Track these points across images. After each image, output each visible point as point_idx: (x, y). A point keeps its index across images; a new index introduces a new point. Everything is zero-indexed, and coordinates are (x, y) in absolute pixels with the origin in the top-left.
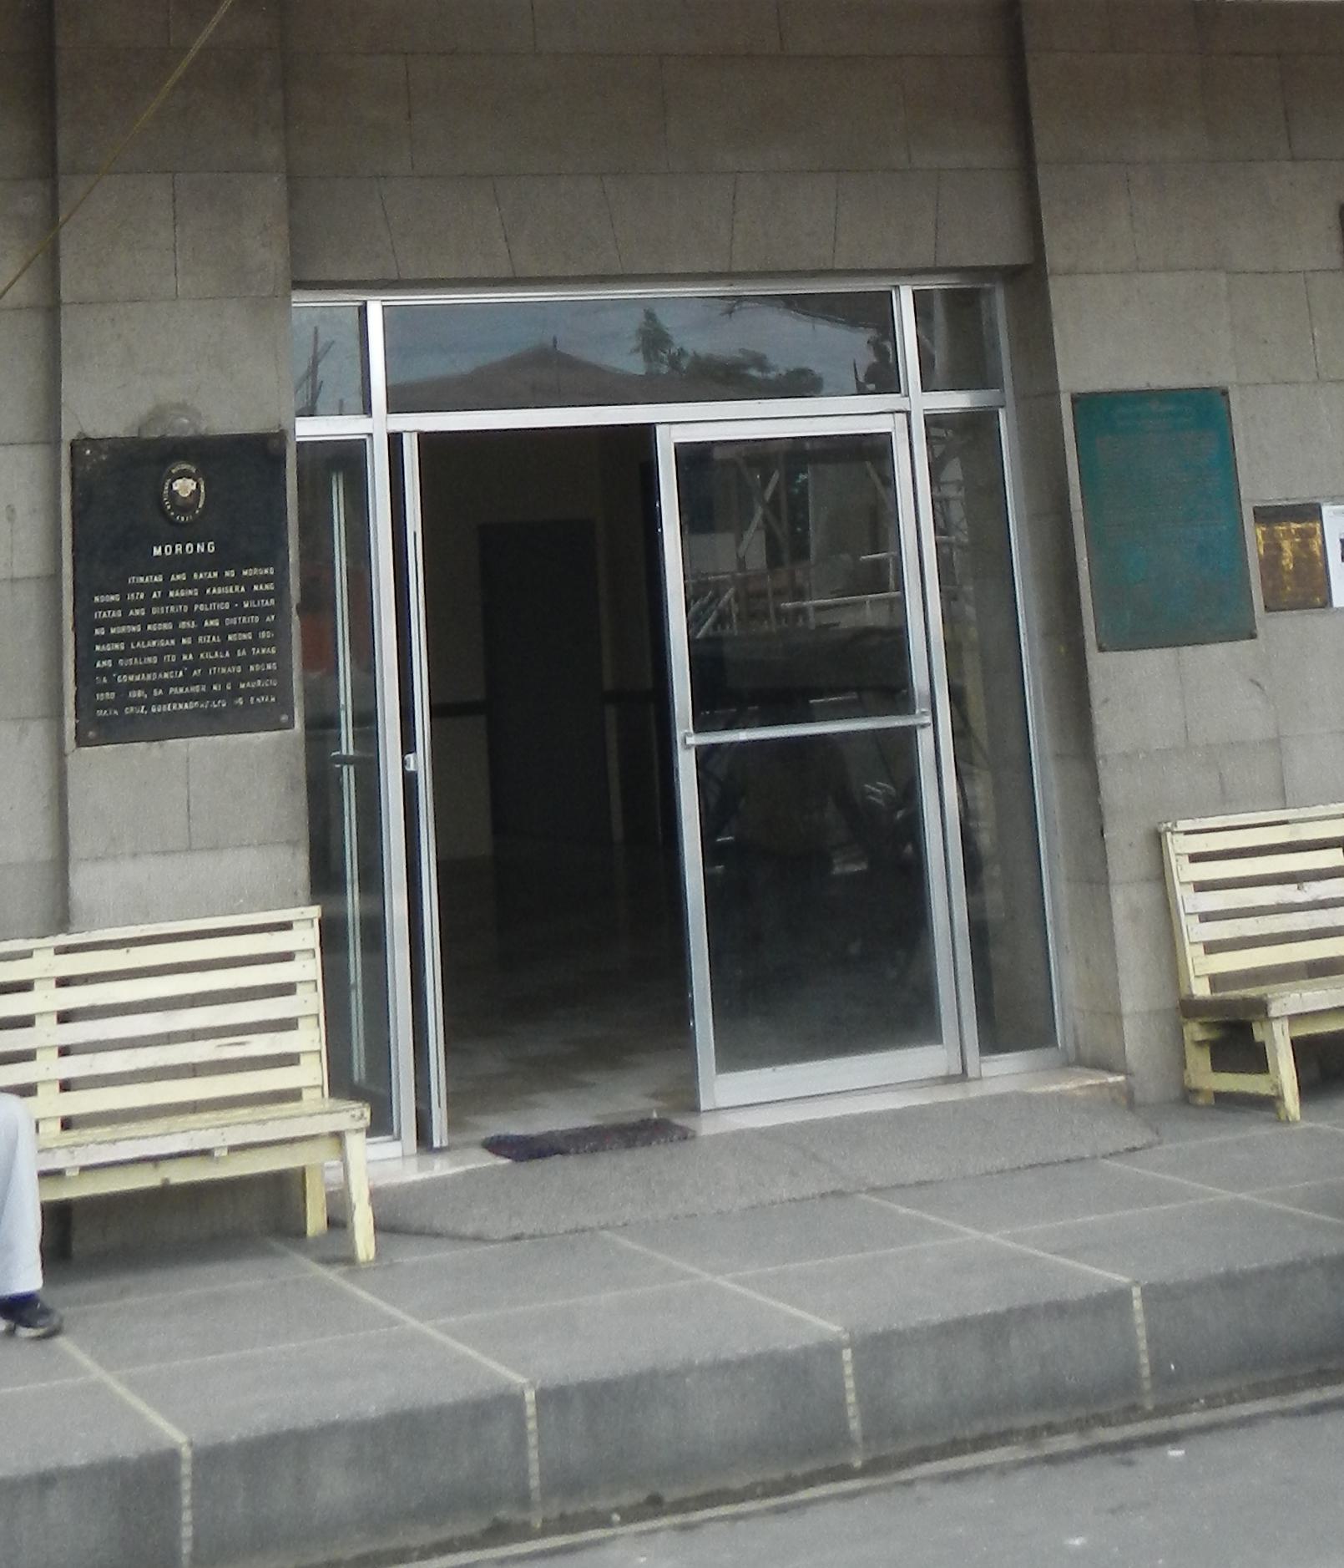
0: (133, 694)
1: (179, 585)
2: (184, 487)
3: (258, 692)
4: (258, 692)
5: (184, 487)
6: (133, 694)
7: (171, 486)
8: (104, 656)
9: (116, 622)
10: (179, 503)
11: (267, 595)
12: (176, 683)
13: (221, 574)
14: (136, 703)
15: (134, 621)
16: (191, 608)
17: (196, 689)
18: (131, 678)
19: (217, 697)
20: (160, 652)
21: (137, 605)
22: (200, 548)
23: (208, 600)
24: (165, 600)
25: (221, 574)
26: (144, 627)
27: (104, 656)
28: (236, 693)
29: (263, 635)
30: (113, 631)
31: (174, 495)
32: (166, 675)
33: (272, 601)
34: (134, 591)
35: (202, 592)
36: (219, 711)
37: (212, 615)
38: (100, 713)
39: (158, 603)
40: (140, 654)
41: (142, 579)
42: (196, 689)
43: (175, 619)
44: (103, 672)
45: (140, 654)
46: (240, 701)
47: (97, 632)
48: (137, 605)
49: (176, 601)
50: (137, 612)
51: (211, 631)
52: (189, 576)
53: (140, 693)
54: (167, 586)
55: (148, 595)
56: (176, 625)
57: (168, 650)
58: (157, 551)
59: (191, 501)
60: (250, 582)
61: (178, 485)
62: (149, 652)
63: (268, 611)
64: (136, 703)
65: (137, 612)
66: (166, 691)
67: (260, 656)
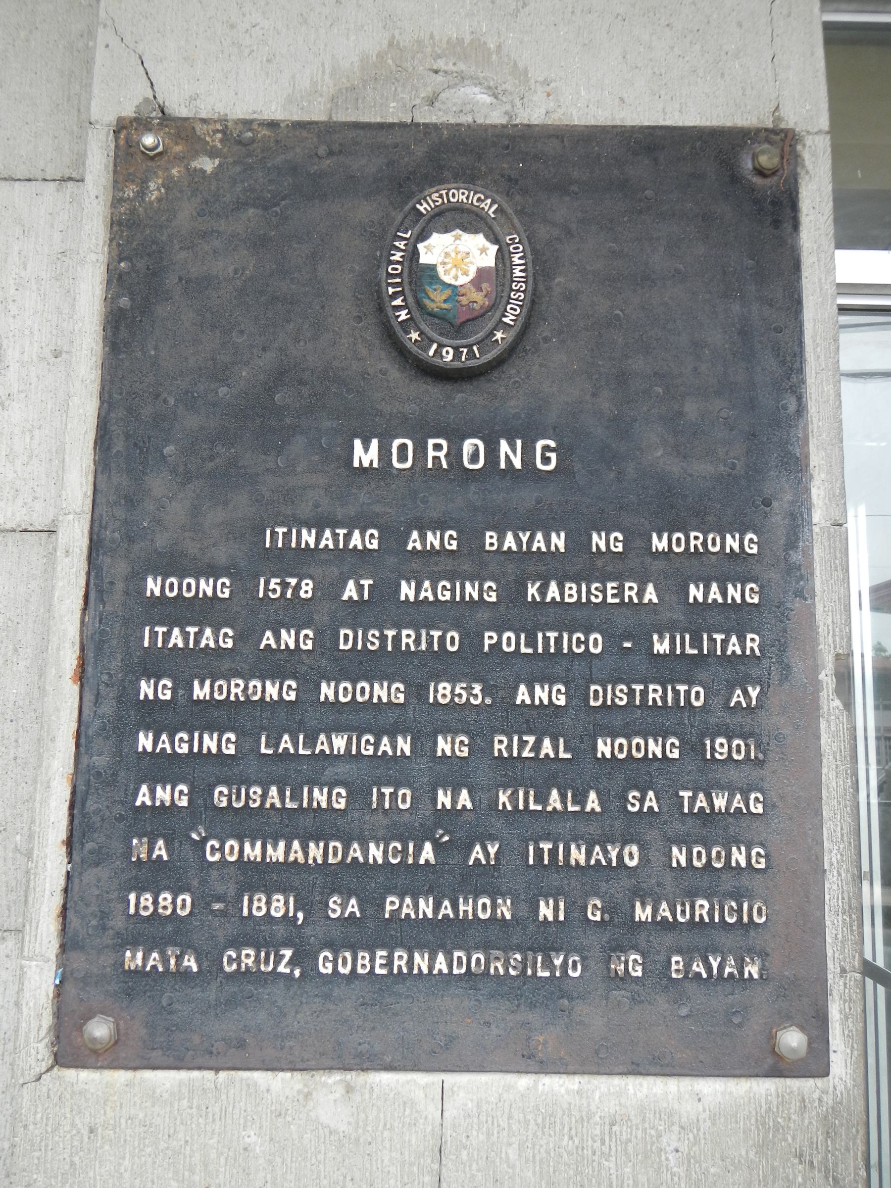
0: (257, 906)
1: (431, 565)
2: (458, 256)
3: (699, 937)
4: (699, 937)
5: (458, 256)
6: (257, 906)
7: (414, 254)
8: (162, 768)
9: (212, 663)
10: (437, 300)
11: (737, 618)
12: (411, 879)
13: (578, 543)
14: (261, 935)
15: (276, 665)
16: (472, 639)
17: (476, 908)
18: (252, 852)
19: (546, 940)
20: (363, 775)
21: (293, 613)
22: (510, 453)
23: (533, 618)
24: (381, 607)
25: (578, 543)
26: (309, 687)
27: (162, 768)
28: (622, 932)
29: (721, 747)
30: (200, 692)
31: (420, 276)
32: (376, 853)
33: (753, 642)
34: (282, 573)
35: (513, 593)
36: (559, 987)
37: (543, 668)
38: (134, 959)
39: (357, 614)
40: (289, 772)
41: (308, 538)
42: (476, 908)
43: (419, 669)
44: (161, 819)
45: (289, 772)
46: (633, 964)
47: (146, 689)
48: (293, 613)
49: (422, 614)
50: (288, 639)
51: (541, 720)
52: (471, 539)
53: (279, 906)
54: (394, 561)
55: (329, 590)
56: (416, 691)
57: (391, 769)
58: (365, 455)
59: (479, 299)
60: (678, 571)
61: (436, 249)
62: (320, 769)
63: (740, 669)
64: (261, 935)
65: (288, 639)
66: (372, 902)
67: (708, 817)
